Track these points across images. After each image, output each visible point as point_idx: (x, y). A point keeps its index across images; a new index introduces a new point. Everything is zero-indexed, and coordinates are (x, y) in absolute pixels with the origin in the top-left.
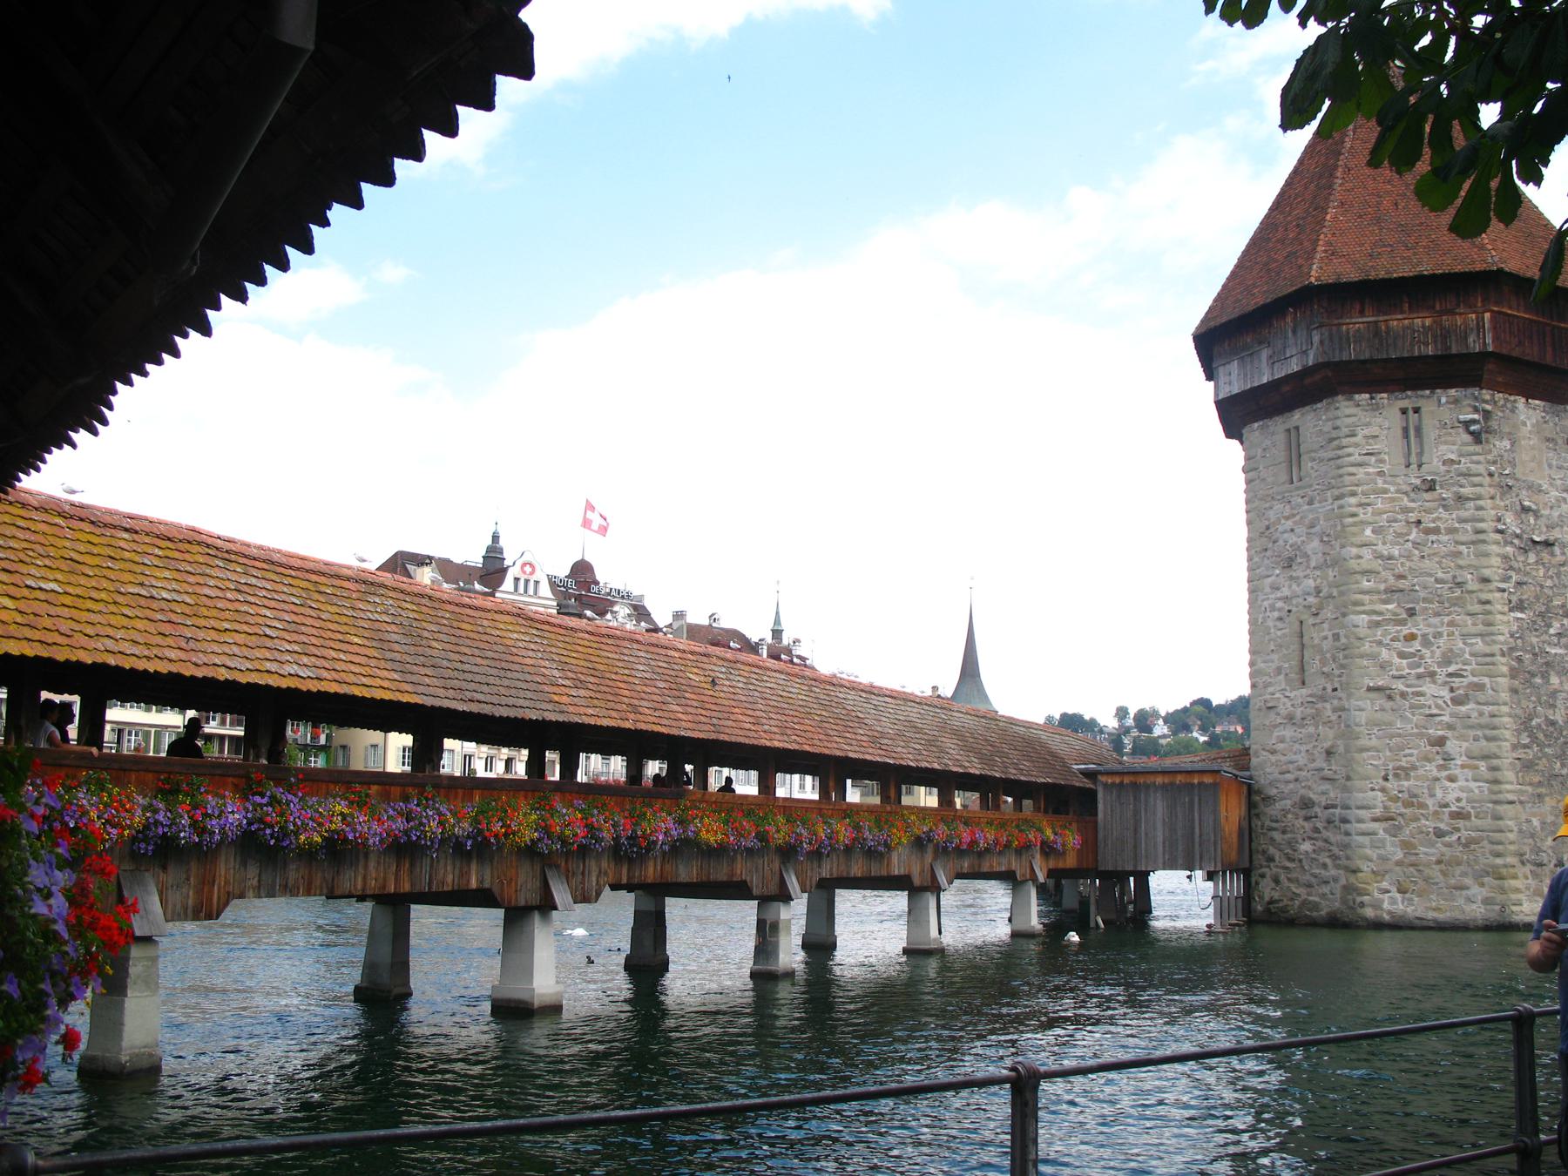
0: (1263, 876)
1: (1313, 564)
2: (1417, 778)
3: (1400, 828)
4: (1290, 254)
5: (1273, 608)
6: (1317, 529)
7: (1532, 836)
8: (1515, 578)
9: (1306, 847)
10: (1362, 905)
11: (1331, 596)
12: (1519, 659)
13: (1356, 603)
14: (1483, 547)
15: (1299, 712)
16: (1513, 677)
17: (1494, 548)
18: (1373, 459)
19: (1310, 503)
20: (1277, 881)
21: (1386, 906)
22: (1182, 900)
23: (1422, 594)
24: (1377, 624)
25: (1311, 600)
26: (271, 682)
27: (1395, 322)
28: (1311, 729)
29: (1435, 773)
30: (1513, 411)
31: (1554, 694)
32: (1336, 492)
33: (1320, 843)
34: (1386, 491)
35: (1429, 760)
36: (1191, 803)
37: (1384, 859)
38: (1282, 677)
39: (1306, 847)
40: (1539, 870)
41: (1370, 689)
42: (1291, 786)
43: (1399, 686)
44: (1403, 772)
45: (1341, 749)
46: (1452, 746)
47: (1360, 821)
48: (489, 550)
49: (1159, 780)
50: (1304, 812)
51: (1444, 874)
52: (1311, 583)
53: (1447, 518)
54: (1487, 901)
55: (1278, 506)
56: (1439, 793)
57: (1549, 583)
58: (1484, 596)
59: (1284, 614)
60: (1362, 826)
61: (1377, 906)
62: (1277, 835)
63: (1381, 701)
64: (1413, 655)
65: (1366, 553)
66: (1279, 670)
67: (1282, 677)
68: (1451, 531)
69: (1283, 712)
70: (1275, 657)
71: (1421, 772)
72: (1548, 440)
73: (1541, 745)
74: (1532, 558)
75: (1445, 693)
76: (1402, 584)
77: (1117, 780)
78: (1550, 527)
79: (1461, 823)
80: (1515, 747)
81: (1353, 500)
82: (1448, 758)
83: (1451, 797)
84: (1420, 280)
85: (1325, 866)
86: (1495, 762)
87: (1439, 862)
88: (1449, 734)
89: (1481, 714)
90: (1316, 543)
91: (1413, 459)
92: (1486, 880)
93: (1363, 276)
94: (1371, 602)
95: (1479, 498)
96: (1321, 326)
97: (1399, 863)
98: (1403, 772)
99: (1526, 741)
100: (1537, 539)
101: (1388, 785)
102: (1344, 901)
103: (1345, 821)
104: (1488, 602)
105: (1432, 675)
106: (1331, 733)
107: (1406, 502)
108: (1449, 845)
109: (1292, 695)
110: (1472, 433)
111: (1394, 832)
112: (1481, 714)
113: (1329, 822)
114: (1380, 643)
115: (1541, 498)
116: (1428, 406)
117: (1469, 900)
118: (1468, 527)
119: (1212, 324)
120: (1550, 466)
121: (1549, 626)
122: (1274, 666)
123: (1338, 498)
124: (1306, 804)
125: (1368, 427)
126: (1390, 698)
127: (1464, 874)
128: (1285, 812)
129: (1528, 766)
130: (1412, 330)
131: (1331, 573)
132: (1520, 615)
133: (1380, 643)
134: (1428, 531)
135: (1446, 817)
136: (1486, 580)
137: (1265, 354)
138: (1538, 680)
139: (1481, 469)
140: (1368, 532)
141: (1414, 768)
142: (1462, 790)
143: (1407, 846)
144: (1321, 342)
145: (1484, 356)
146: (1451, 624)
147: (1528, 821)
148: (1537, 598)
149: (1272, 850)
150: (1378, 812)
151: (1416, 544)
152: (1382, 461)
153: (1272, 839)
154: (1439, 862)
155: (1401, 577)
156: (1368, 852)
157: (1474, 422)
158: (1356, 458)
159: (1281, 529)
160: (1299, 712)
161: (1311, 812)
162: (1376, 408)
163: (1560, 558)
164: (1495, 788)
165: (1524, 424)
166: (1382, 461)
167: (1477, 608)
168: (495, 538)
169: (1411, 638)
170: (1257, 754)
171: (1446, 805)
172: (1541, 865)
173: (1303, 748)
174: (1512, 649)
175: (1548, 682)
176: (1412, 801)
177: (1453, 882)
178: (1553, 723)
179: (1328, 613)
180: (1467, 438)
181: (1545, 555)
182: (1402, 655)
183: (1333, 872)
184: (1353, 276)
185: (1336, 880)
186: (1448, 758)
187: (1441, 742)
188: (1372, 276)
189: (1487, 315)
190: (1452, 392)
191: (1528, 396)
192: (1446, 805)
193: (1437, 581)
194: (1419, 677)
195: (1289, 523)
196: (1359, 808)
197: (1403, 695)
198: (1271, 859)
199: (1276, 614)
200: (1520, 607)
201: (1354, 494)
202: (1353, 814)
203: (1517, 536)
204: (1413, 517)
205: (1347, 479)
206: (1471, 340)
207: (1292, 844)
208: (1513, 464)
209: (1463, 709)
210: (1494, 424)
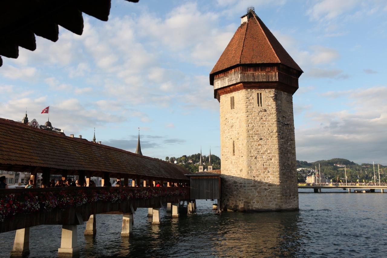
0: (224, 199)
1: (237, 128)
3: (257, 188)
4: (233, 56)
7: (285, 190)
8: (282, 132)
11: (241, 135)
12: (282, 150)
16: (281, 154)
18: (251, 104)
21: (254, 206)
27: (256, 73)
30: (281, 94)
31: (289, 158)
36: (213, 183)
38: (229, 153)
40: (286, 197)
45: (244, 170)
47: (248, 187)
49: (205, 178)
54: (276, 204)
57: (288, 133)
60: (248, 188)
61: (252, 206)
67: (229, 153)
72: (288, 101)
74: (285, 128)
76: (257, 133)
77: (195, 178)
78: (288, 121)
79: (270, 187)
90: (238, 123)
92: (276, 200)
93: (251, 63)
97: (257, 196)
99: (284, 168)
100: (286, 123)
103: (244, 187)
108: (269, 192)
109: (232, 158)
111: (256, 189)
113: (241, 187)
117: (272, 204)
119: (215, 72)
120: (288, 107)
122: (227, 151)
127: (271, 199)
128: (230, 184)
132: (282, 140)
134: (263, 121)
135: (267, 186)
137: (227, 79)
138: (286, 155)
142: (271, 179)
143: (258, 192)
144: (241, 77)
145: (276, 82)
147: (284, 186)
148: (286, 136)
149: (227, 193)
152: (253, 105)
154: (266, 196)
155: (257, 131)
156: (250, 193)
160: (233, 161)
163: (290, 128)
165: (283, 98)
170: (223, 170)
172: (286, 196)
175: (288, 155)
178: (288, 164)
183: (242, 198)
184: (248, 62)
185: (243, 200)
189: (277, 73)
190: (269, 90)
191: (284, 91)
196: (248, 184)
199: (228, 139)
203: (282, 123)
206: (274, 78)
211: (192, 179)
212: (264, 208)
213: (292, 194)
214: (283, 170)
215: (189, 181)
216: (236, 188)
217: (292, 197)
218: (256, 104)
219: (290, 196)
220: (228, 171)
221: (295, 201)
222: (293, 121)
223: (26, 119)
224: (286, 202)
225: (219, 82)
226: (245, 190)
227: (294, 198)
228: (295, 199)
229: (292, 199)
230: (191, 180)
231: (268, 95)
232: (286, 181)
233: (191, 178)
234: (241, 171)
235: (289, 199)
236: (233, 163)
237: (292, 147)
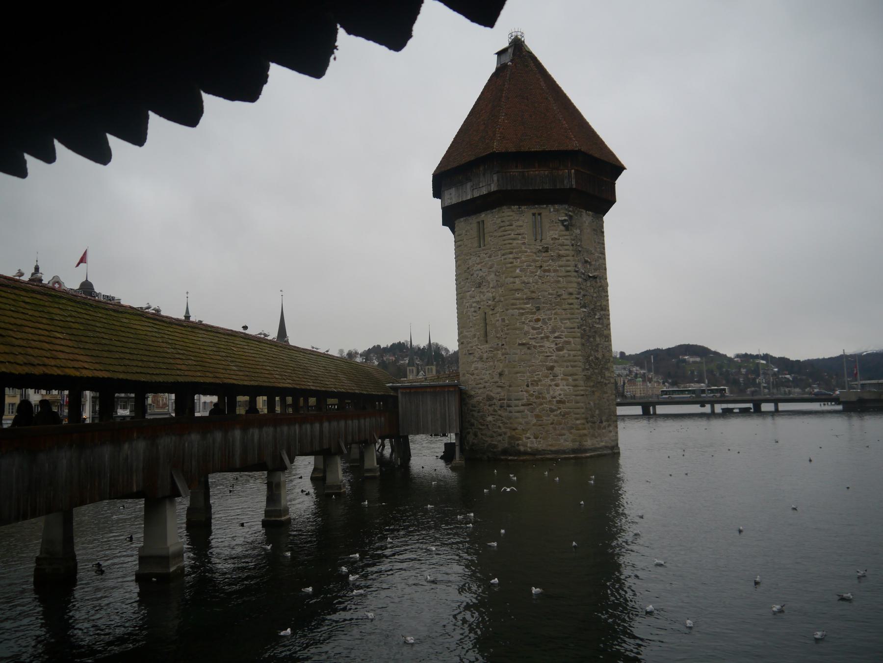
0: (469, 433)
1: (491, 286)
2: (541, 385)
5: (471, 307)
6: (493, 269)
7: (591, 410)
8: (582, 293)
9: (490, 418)
10: (518, 445)
13: (513, 304)
14: (569, 279)
15: (485, 356)
17: (574, 279)
19: (490, 257)
20: (476, 435)
23: (542, 300)
24: (522, 314)
26: (47, 371)
28: (491, 364)
29: (549, 383)
32: (503, 252)
33: (497, 417)
34: (526, 252)
35: (547, 377)
37: (527, 423)
39: (490, 418)
41: (519, 344)
42: (481, 390)
43: (533, 342)
44: (536, 383)
45: (506, 373)
46: (557, 370)
47: (516, 406)
49: (428, 390)
50: (488, 403)
51: (555, 429)
52: (490, 295)
54: (574, 441)
55: (474, 258)
56: (551, 393)
58: (570, 301)
59: (477, 309)
60: (517, 408)
62: (476, 414)
63: (525, 350)
64: (538, 328)
65: (517, 281)
66: (474, 336)
68: (555, 271)
69: (477, 355)
70: (473, 329)
71: (543, 382)
72: (594, 230)
74: (589, 284)
75: (553, 346)
76: (534, 295)
78: (595, 270)
79: (561, 405)
80: (583, 370)
81: (511, 256)
82: (555, 376)
84: (544, 153)
85: (499, 427)
86: (576, 377)
87: (552, 424)
88: (555, 364)
89: (569, 355)
90: (492, 276)
94: (520, 304)
95: (567, 256)
96: (498, 172)
97: (534, 425)
98: (536, 383)
101: (529, 389)
103: (509, 406)
104: (572, 304)
105: (547, 337)
106: (501, 365)
107: (535, 257)
108: (556, 416)
110: (564, 226)
112: (569, 355)
113: (501, 407)
114: (524, 323)
116: (545, 213)
117: (566, 440)
119: (443, 169)
121: (595, 315)
123: (503, 255)
124: (490, 398)
125: (517, 221)
126: (529, 348)
127: (563, 429)
128: (479, 402)
129: (588, 378)
130: (539, 177)
131: (500, 290)
133: (524, 323)
134: (545, 271)
136: (571, 294)
137: (469, 185)
139: (568, 242)
140: (518, 271)
141: (540, 380)
142: (561, 390)
143: (537, 416)
145: (571, 189)
146: (555, 314)
149: (473, 421)
150: (524, 401)
151: (540, 277)
152: (524, 238)
153: (473, 415)
154: (552, 424)
155: (533, 292)
156: (521, 420)
157: (565, 220)
158: (512, 236)
159: (475, 269)
160: (485, 356)
161: (492, 402)
162: (522, 213)
163: (599, 284)
164: (576, 389)
166: (524, 238)
167: (567, 306)
169: (538, 320)
170: (464, 375)
171: (555, 397)
172: (594, 423)
173: (488, 372)
174: (582, 325)
176: (540, 396)
177: (558, 432)
178: (597, 359)
179: (499, 309)
180: (562, 228)
181: (593, 282)
182: (534, 329)
183: (504, 430)
184: (512, 149)
185: (505, 433)
186: (555, 376)
187: (552, 368)
188: (523, 149)
189: (573, 171)
190: (557, 207)
192: (555, 397)
193: (549, 294)
194: (542, 338)
195: (479, 267)
197: (535, 347)
198: (472, 425)
199: (473, 309)
200: (585, 307)
201: (511, 253)
202: (514, 402)
204: (538, 264)
206: (565, 182)
208: (581, 240)
209: (561, 353)
210: (573, 222)
211: (402, 393)
213: (604, 418)
214: (587, 369)
215: (397, 397)
216: (491, 409)
217: (604, 424)
219: (601, 422)
220: (475, 376)
221: (610, 432)
223: (187, 317)
224: (593, 436)
226: (510, 412)
227: (609, 425)
228: (611, 428)
229: (604, 428)
230: (400, 395)
231: (553, 216)
232: (593, 392)
233: (399, 391)
234: (501, 374)
235: (599, 428)
236: (484, 359)
237: (602, 324)
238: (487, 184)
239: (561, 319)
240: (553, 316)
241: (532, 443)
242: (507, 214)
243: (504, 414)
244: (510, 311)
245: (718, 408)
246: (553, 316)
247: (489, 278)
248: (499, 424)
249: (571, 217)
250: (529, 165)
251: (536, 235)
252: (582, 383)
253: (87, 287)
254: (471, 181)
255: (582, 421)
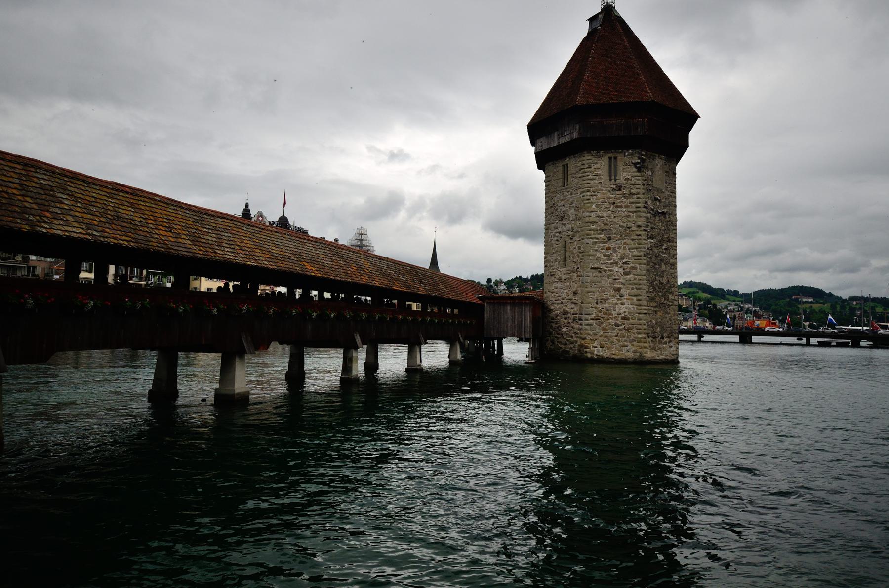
7: (653, 326)
9: (564, 329)
10: (586, 352)
11: (578, 232)
12: (651, 258)
13: (588, 235)
15: (563, 277)
22: (516, 351)
24: (596, 243)
25: (570, 233)
31: (663, 272)
35: (614, 296)
37: (595, 334)
39: (564, 329)
43: (603, 267)
47: (586, 320)
48: (244, 210)
51: (618, 341)
53: (627, 201)
54: (635, 352)
55: (558, 196)
56: (617, 310)
58: (638, 233)
61: (592, 353)
62: (554, 325)
63: (596, 273)
65: (592, 214)
68: (627, 207)
73: (657, 292)
74: (657, 218)
75: (621, 270)
76: (606, 227)
78: (665, 207)
79: (626, 321)
80: (647, 292)
81: (588, 194)
82: (622, 296)
83: (621, 311)
85: (572, 337)
90: (573, 210)
91: (613, 178)
95: (638, 194)
98: (604, 301)
102: (579, 350)
103: (580, 319)
105: (616, 263)
111: (600, 324)
115: (663, 195)
116: (620, 157)
117: (627, 351)
118: (633, 205)
124: (565, 313)
125: (596, 167)
126: (600, 272)
127: (626, 341)
129: (652, 299)
134: (618, 207)
136: (639, 227)
139: (639, 182)
141: (608, 299)
143: (604, 329)
146: (625, 243)
150: (594, 316)
157: (638, 163)
158: (590, 177)
160: (563, 277)
162: (600, 157)
167: (635, 237)
168: (247, 205)
169: (609, 248)
172: (655, 338)
178: (662, 283)
179: (576, 238)
180: (635, 170)
182: (605, 255)
185: (576, 342)
186: (622, 296)
187: (619, 289)
194: (612, 264)
197: (605, 271)
198: (551, 334)
200: (652, 238)
201: (589, 191)
202: (584, 317)
204: (612, 201)
205: (586, 185)
207: (559, 328)
212: (613, 356)
218: (605, 177)
219: (662, 338)
222: (675, 206)
224: (653, 349)
225: (543, 139)
229: (665, 343)
232: (656, 312)
234: (575, 293)
235: (660, 343)
237: (669, 254)
238: (571, 134)
239: (630, 248)
240: (622, 246)
241: (598, 351)
242: (587, 158)
243: (576, 326)
244: (586, 240)
245: (814, 341)
246: (622, 246)
247: (570, 213)
248: (572, 334)
249: (643, 161)
250: (612, 115)
251: (610, 176)
252: (645, 303)
253: (283, 221)
254: (557, 130)
255: (644, 336)
